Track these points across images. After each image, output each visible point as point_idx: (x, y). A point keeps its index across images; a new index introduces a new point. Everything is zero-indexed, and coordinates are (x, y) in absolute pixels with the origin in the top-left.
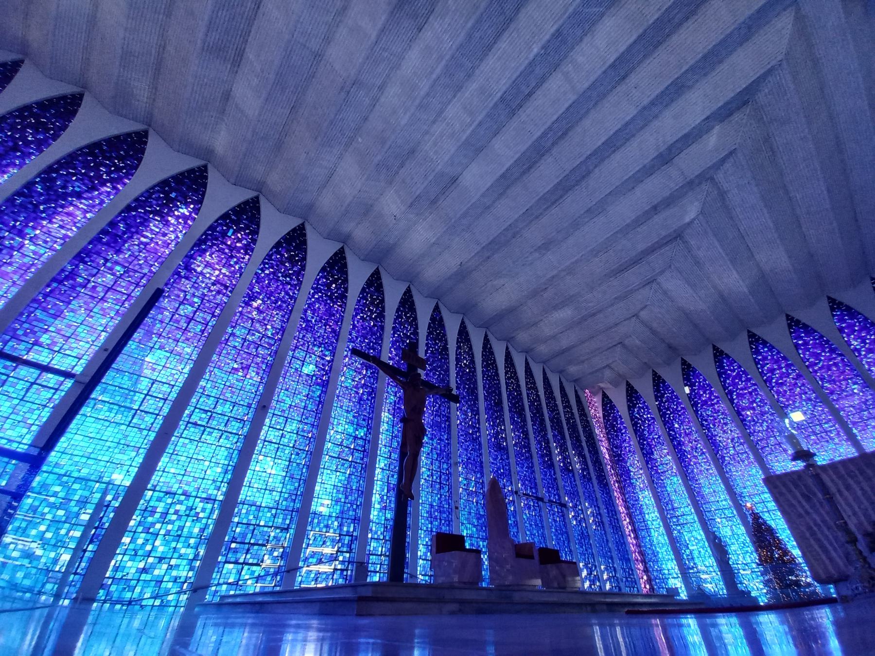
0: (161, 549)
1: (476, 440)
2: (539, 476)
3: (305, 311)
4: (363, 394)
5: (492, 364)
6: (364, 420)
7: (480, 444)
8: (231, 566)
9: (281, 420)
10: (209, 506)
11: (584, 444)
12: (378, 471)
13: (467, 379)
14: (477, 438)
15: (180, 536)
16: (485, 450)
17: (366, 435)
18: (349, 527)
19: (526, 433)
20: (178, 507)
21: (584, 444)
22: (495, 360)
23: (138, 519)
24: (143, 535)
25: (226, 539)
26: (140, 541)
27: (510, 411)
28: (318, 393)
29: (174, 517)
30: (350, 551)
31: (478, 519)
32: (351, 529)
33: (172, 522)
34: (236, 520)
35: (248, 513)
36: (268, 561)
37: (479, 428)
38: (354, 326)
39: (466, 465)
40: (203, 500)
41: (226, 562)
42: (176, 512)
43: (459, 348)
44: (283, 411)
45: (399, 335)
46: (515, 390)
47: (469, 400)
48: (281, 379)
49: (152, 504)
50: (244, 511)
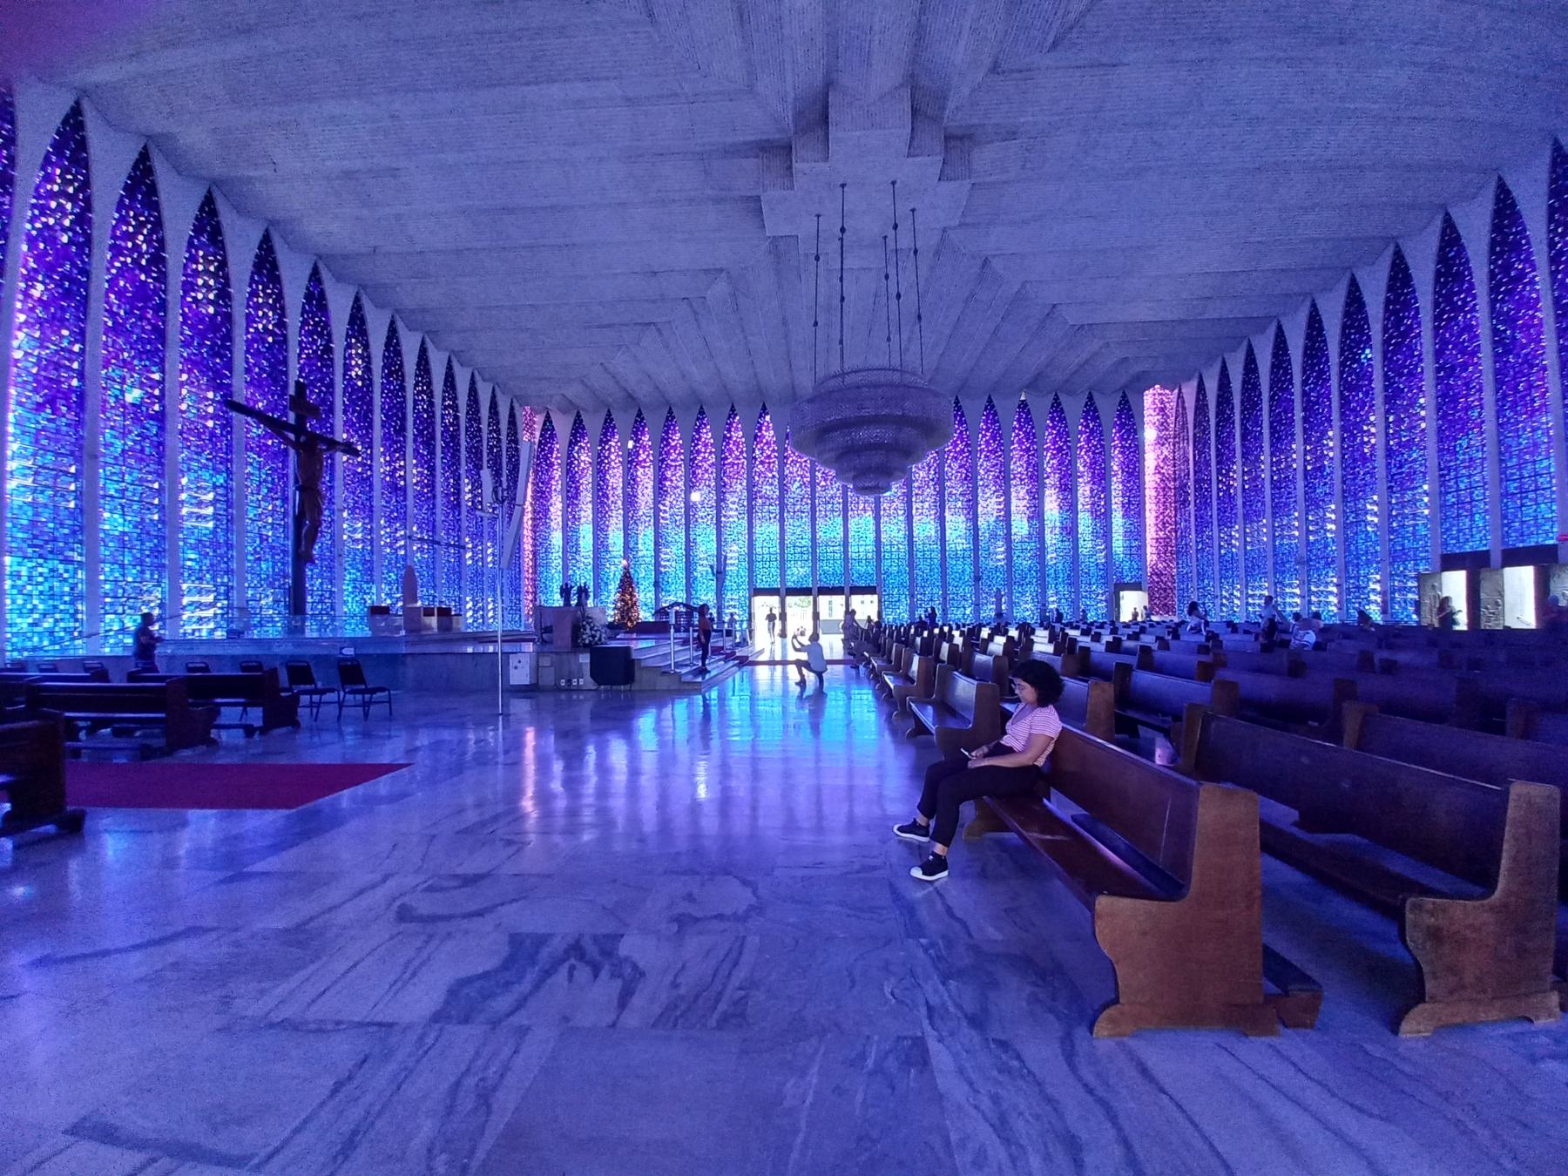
1: (367, 481)
5: (396, 372)
7: (371, 486)
13: (358, 398)
16: (377, 493)
19: (432, 469)
22: (401, 366)
29: (40, 579)
35: (112, 570)
37: (371, 467)
39: (352, 511)
40: (61, 562)
42: (41, 574)
46: (425, 411)
47: (361, 428)
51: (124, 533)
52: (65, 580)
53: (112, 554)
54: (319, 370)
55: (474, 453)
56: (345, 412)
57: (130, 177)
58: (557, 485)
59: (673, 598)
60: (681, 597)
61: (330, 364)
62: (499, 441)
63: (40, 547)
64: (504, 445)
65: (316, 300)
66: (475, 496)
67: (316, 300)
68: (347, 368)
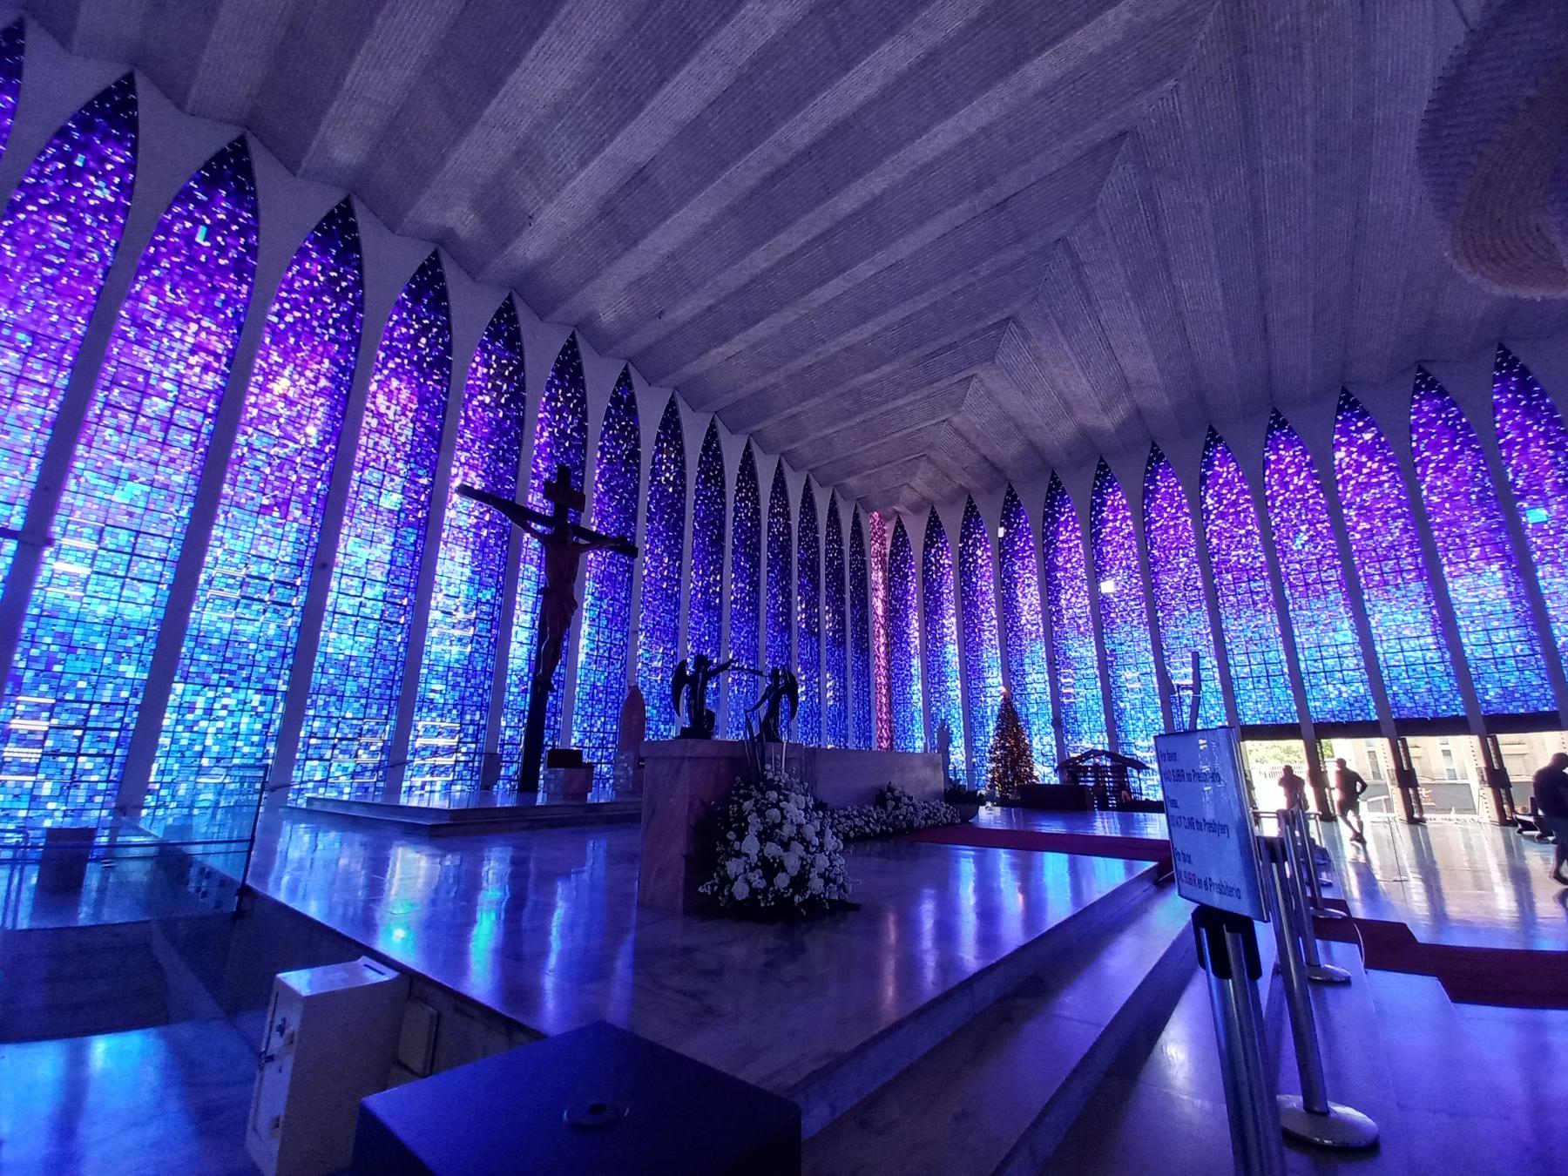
0: (216, 749)
1: (672, 599)
2: (764, 641)
4: (488, 537)
5: (715, 477)
6: (491, 576)
7: (678, 603)
8: (316, 763)
9: (356, 582)
10: (270, 698)
11: (847, 596)
12: (514, 646)
13: (668, 506)
14: (674, 595)
15: (237, 734)
16: (684, 611)
17: (494, 597)
20: (225, 701)
21: (847, 596)
22: (722, 471)
23: (174, 716)
24: (187, 735)
25: (302, 734)
26: (184, 742)
27: (734, 552)
28: (412, 539)
29: (224, 713)
31: (661, 700)
32: (477, 717)
33: (223, 719)
34: (311, 712)
35: (326, 704)
36: (364, 756)
37: (678, 581)
39: (651, 633)
40: (258, 691)
41: (307, 759)
42: (225, 707)
43: (660, 450)
44: (357, 569)
47: (668, 538)
49: (187, 698)
50: (320, 702)
52: (259, 715)
53: (330, 682)
54: (623, 475)
55: (809, 567)
58: (914, 600)
59: (1086, 745)
60: (1101, 742)
61: (635, 470)
62: (841, 552)
63: (232, 673)
64: (847, 558)
65: (624, 405)
66: (809, 617)
67: (624, 405)
68: (655, 473)
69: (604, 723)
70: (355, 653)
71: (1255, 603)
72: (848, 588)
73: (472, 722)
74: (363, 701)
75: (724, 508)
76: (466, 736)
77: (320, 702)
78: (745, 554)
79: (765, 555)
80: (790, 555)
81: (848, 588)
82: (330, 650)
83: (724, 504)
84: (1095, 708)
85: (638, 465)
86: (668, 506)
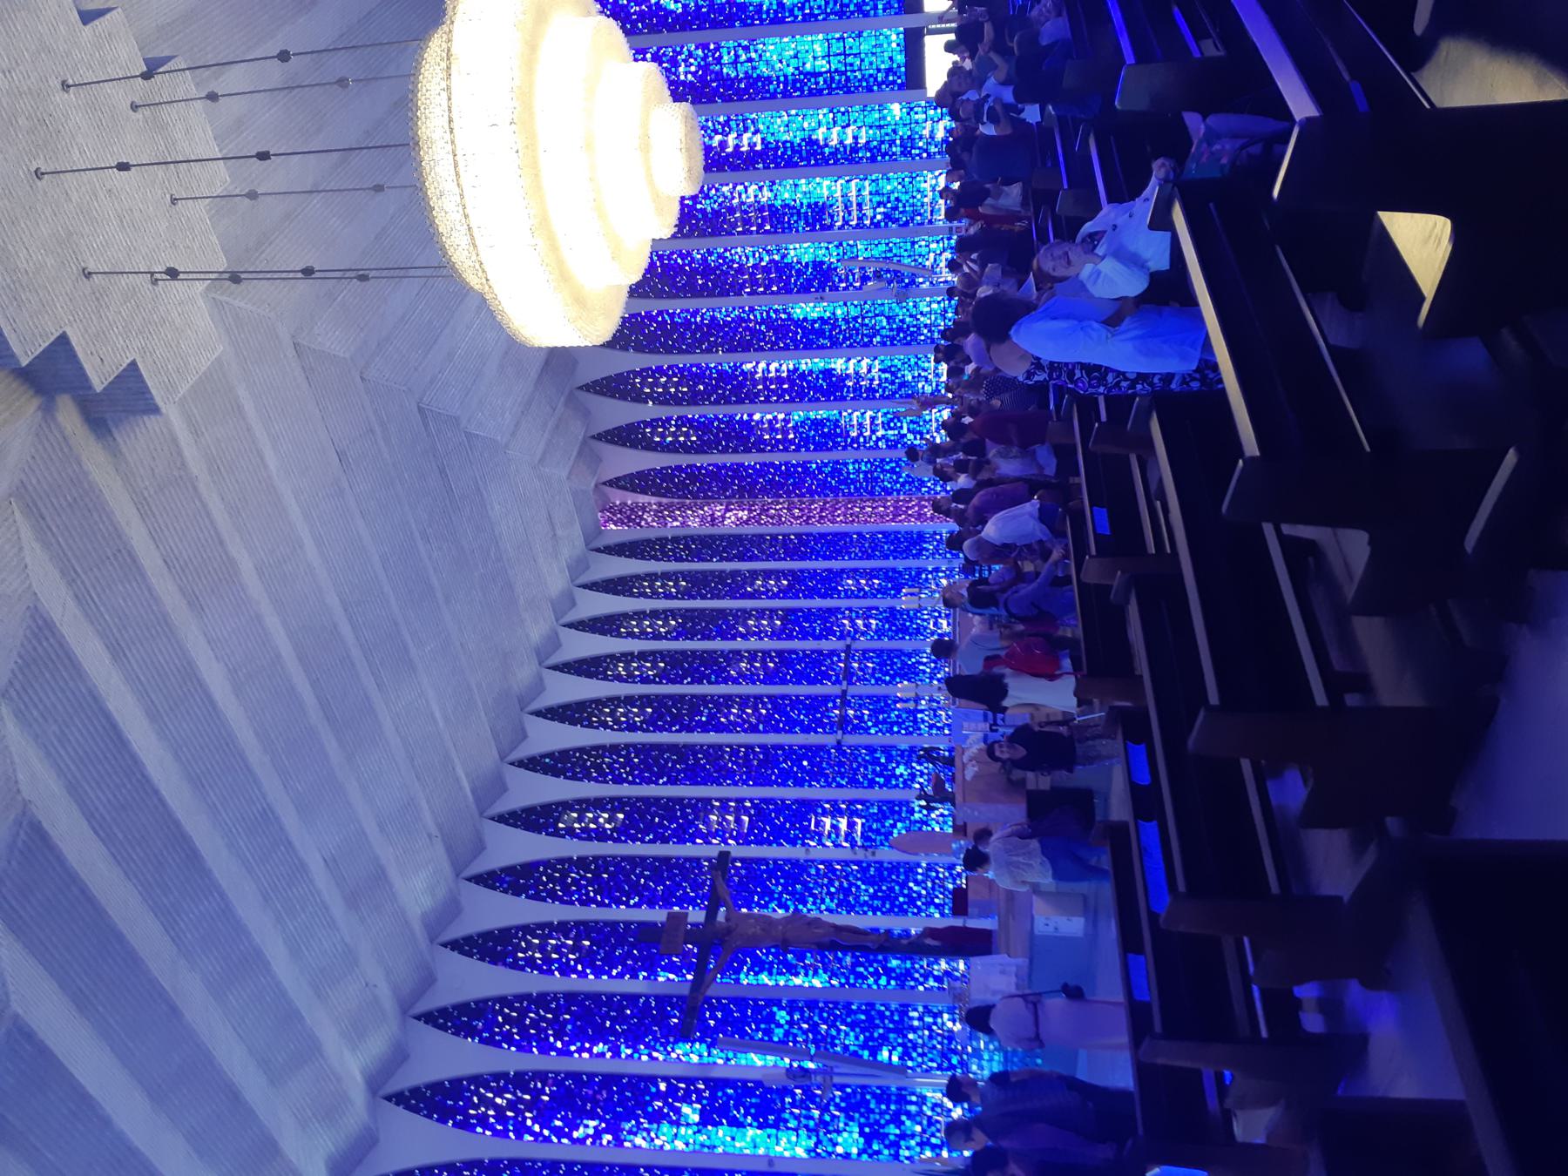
3: (574, 1141)
11: (728, 566)
18: (912, 1019)
21: (728, 566)
30: (940, 1014)
32: (915, 1014)
35: (908, 1148)
38: (580, 1050)
45: (577, 961)
48: (720, 1150)
51: (862, 1133)
53: (887, 1147)
56: (665, 841)
57: (429, 1116)
68: (601, 835)
69: (917, 883)
70: (857, 1129)
71: (750, 60)
72: (715, 565)
73: (920, 1019)
74: (904, 1118)
75: (634, 746)
76: (935, 1023)
77: (907, 1153)
78: (692, 715)
79: (686, 689)
80: (683, 652)
81: (715, 565)
82: (855, 1151)
83: (627, 746)
84: (883, 248)
85: (596, 859)
86: (642, 818)
